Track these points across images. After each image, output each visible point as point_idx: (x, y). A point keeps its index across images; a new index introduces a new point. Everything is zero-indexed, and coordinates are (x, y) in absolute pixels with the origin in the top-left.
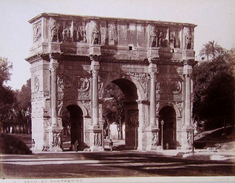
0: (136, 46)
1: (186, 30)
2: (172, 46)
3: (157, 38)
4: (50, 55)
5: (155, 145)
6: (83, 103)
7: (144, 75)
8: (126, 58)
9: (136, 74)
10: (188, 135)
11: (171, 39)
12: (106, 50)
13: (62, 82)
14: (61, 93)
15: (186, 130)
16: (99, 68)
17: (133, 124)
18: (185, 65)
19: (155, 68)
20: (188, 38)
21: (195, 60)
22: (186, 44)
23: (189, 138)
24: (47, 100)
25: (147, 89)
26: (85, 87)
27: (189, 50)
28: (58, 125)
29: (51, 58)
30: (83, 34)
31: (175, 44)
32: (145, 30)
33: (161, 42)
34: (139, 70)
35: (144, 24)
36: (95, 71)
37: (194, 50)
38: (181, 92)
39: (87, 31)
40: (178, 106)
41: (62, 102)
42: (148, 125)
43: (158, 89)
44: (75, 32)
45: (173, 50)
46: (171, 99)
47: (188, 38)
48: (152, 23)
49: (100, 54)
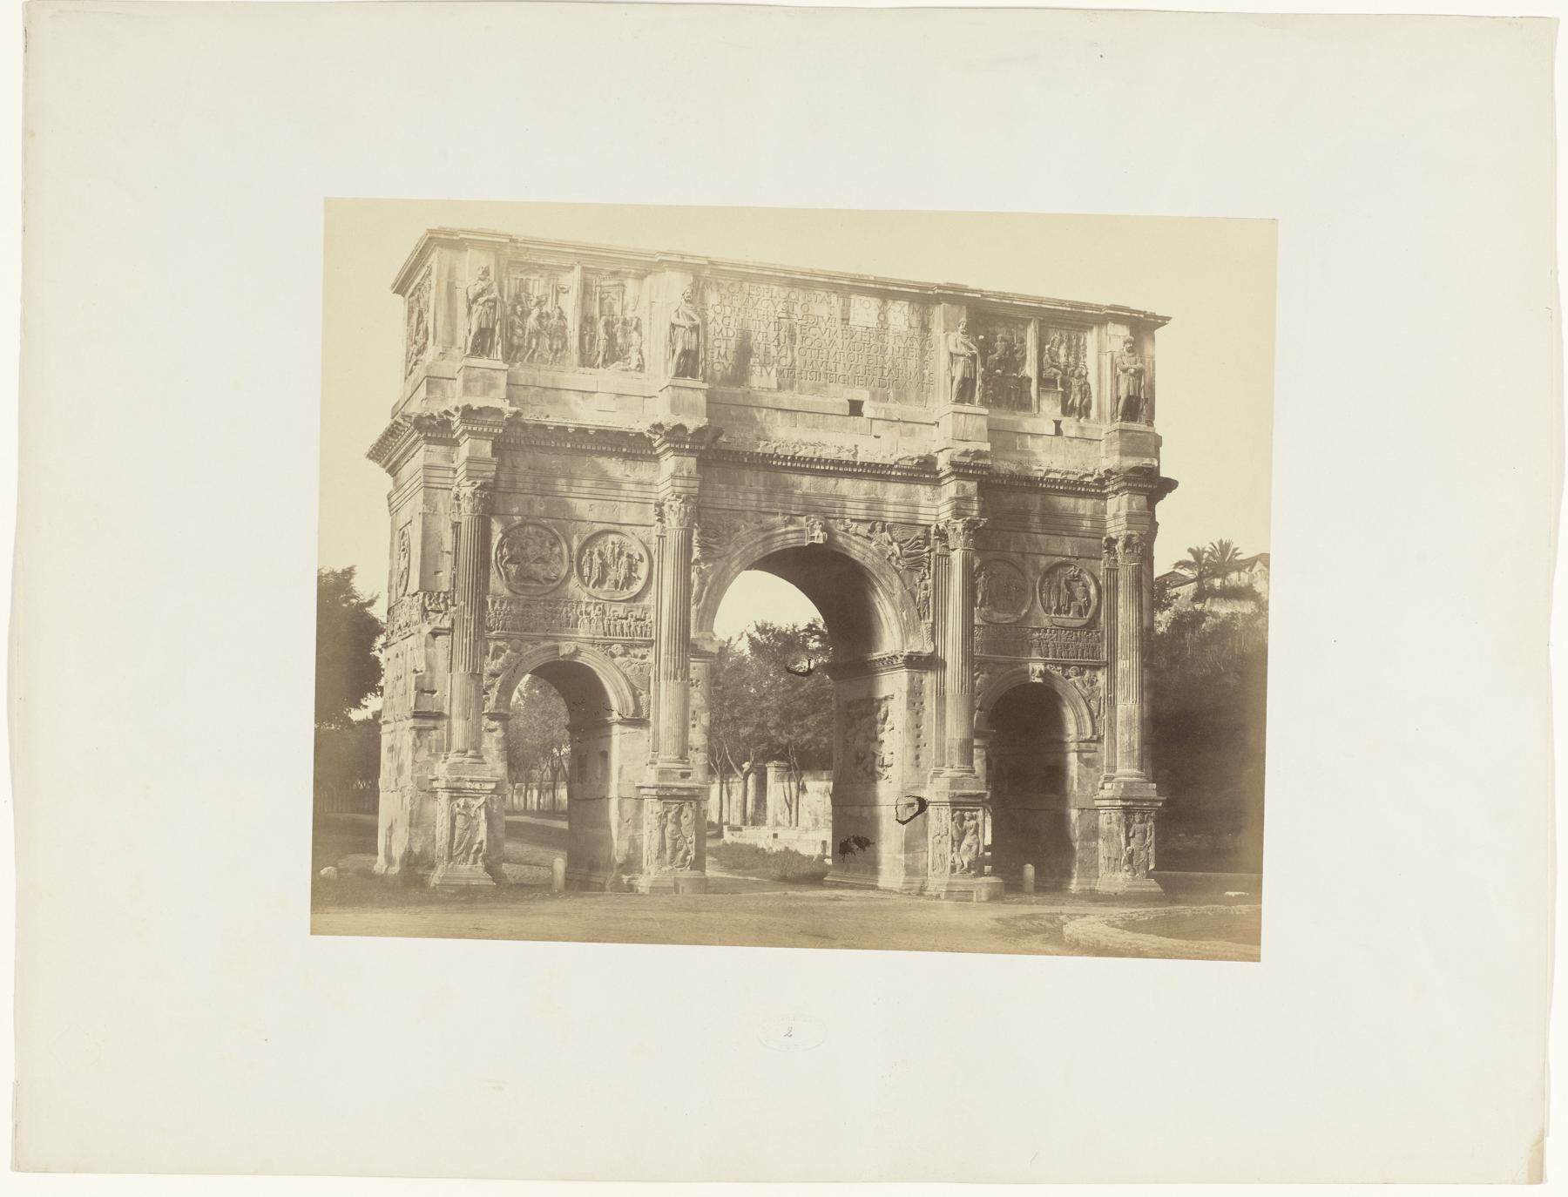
2: (1050, 408)
4: (456, 420)
5: (969, 870)
6: (613, 656)
8: (829, 453)
11: (1047, 373)
15: (1119, 803)
17: (865, 769)
18: (1116, 493)
20: (1125, 371)
22: (1118, 399)
26: (629, 580)
28: (481, 757)
35: (924, 298)
36: (676, 504)
37: (1159, 427)
38: (1092, 624)
44: (587, 321)
45: (1058, 423)
47: (1125, 371)
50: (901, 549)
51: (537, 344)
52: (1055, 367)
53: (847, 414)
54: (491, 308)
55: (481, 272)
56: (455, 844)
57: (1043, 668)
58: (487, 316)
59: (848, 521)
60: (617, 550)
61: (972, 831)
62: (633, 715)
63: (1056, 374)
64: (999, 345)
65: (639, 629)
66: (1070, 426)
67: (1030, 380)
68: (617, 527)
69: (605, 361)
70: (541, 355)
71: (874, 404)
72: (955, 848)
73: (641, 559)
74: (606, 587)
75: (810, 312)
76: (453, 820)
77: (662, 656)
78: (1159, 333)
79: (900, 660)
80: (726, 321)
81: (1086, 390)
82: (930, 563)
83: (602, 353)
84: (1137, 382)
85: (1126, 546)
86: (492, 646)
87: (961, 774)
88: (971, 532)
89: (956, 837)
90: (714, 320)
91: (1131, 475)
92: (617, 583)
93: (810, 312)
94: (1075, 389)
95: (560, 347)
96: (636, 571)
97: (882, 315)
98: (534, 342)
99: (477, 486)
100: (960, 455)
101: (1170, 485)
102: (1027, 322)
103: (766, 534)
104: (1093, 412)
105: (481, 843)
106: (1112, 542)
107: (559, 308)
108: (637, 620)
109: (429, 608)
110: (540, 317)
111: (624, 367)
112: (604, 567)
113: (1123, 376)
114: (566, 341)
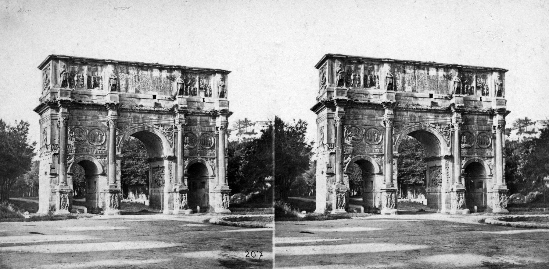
3: (185, 85)
7: (170, 127)
10: (222, 197)
11: (201, 87)
13: (73, 134)
14: (72, 146)
20: (220, 85)
21: (230, 111)
24: (55, 154)
26: (101, 141)
29: (60, 106)
30: (98, 80)
31: (205, 92)
33: (190, 90)
39: (103, 77)
41: (73, 157)
43: (186, 144)
44: (89, 77)
45: (204, 99)
46: (203, 155)
66: (207, 99)
69: (94, 87)
78: (229, 75)
85: (221, 129)
94: (208, 90)
104: (213, 96)
106: (217, 128)
113: (220, 87)
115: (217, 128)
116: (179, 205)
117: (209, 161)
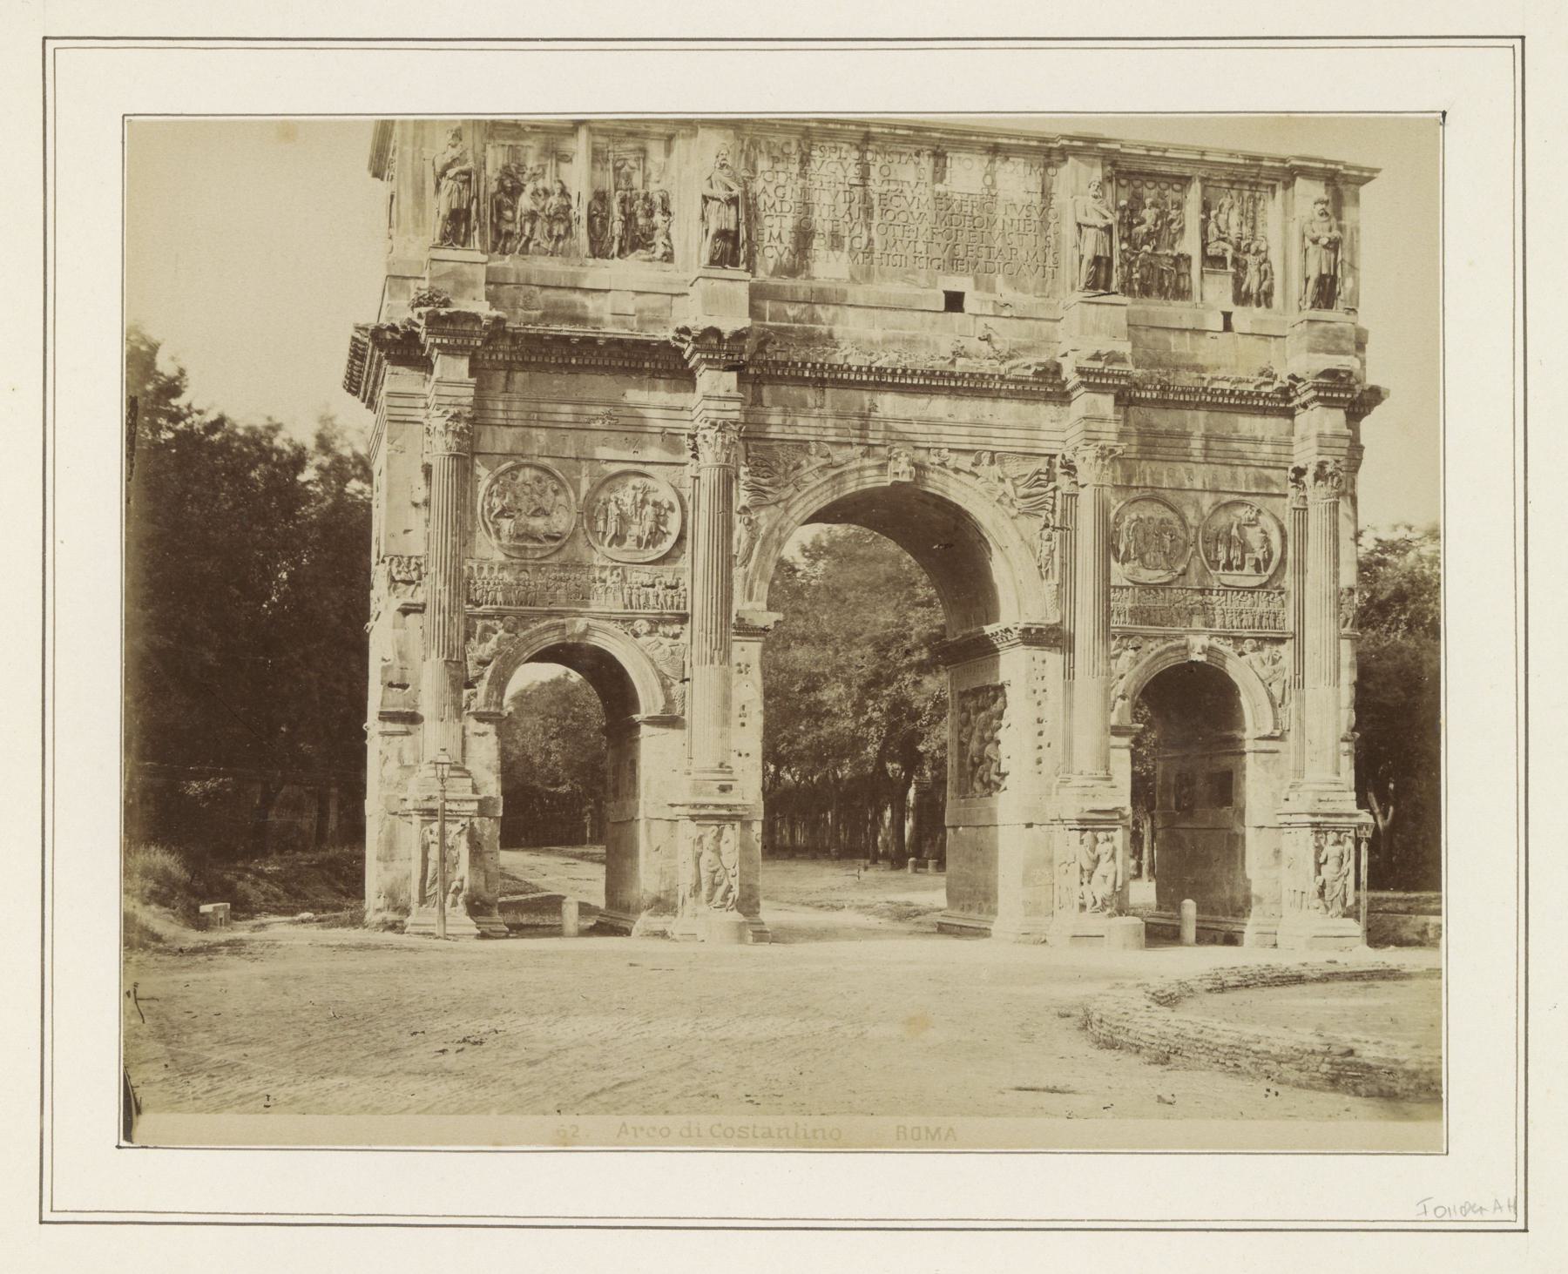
0: (991, 289)
1: (1309, 193)
4: (422, 331)
5: (1104, 906)
7: (1042, 465)
8: (921, 359)
9: (986, 461)
10: (1319, 849)
11: (1211, 251)
12: (792, 311)
16: (736, 415)
19: (1103, 420)
20: (1315, 242)
21: (1371, 380)
22: (1307, 280)
23: (1329, 871)
25: (1057, 555)
27: (1325, 314)
31: (1238, 282)
32: (1046, 193)
34: (1010, 433)
40: (1257, 664)
42: (1065, 782)
45: (1227, 316)
47: (1315, 242)
48: (1086, 147)
49: (744, 322)
50: (1016, 487)
51: (532, 230)
52: (1224, 240)
53: (942, 307)
54: (463, 182)
55: (450, 136)
56: (428, 883)
57: (1207, 643)
58: (459, 192)
59: (945, 452)
60: (640, 497)
61: (1108, 857)
62: (664, 711)
63: (1225, 250)
64: (1149, 214)
65: (669, 599)
66: (1244, 318)
67: (1188, 259)
68: (640, 468)
69: (621, 251)
70: (538, 245)
71: (978, 294)
72: (1085, 880)
73: (671, 509)
74: (625, 546)
75: (891, 177)
76: (425, 849)
77: (696, 639)
79: (1016, 633)
80: (780, 192)
81: (1266, 272)
82: (1054, 505)
83: (617, 240)
84: (1333, 256)
85: (1317, 477)
86: (480, 624)
87: (1090, 783)
88: (1107, 462)
89: (1087, 865)
90: (764, 191)
91: (1321, 380)
92: (639, 540)
93: (891, 177)
94: (1252, 269)
95: (562, 233)
96: (665, 524)
97: (988, 178)
98: (528, 226)
99: (448, 416)
100: (1089, 359)
101: (1375, 396)
102: (1185, 181)
103: (836, 472)
105: (462, 880)
106: (1300, 472)
107: (561, 182)
108: (667, 587)
109: (397, 578)
110: (535, 193)
111: (647, 257)
112: (623, 519)
114: (570, 226)
115: (1300, 472)
116: (1078, 891)
117: (1251, 656)
